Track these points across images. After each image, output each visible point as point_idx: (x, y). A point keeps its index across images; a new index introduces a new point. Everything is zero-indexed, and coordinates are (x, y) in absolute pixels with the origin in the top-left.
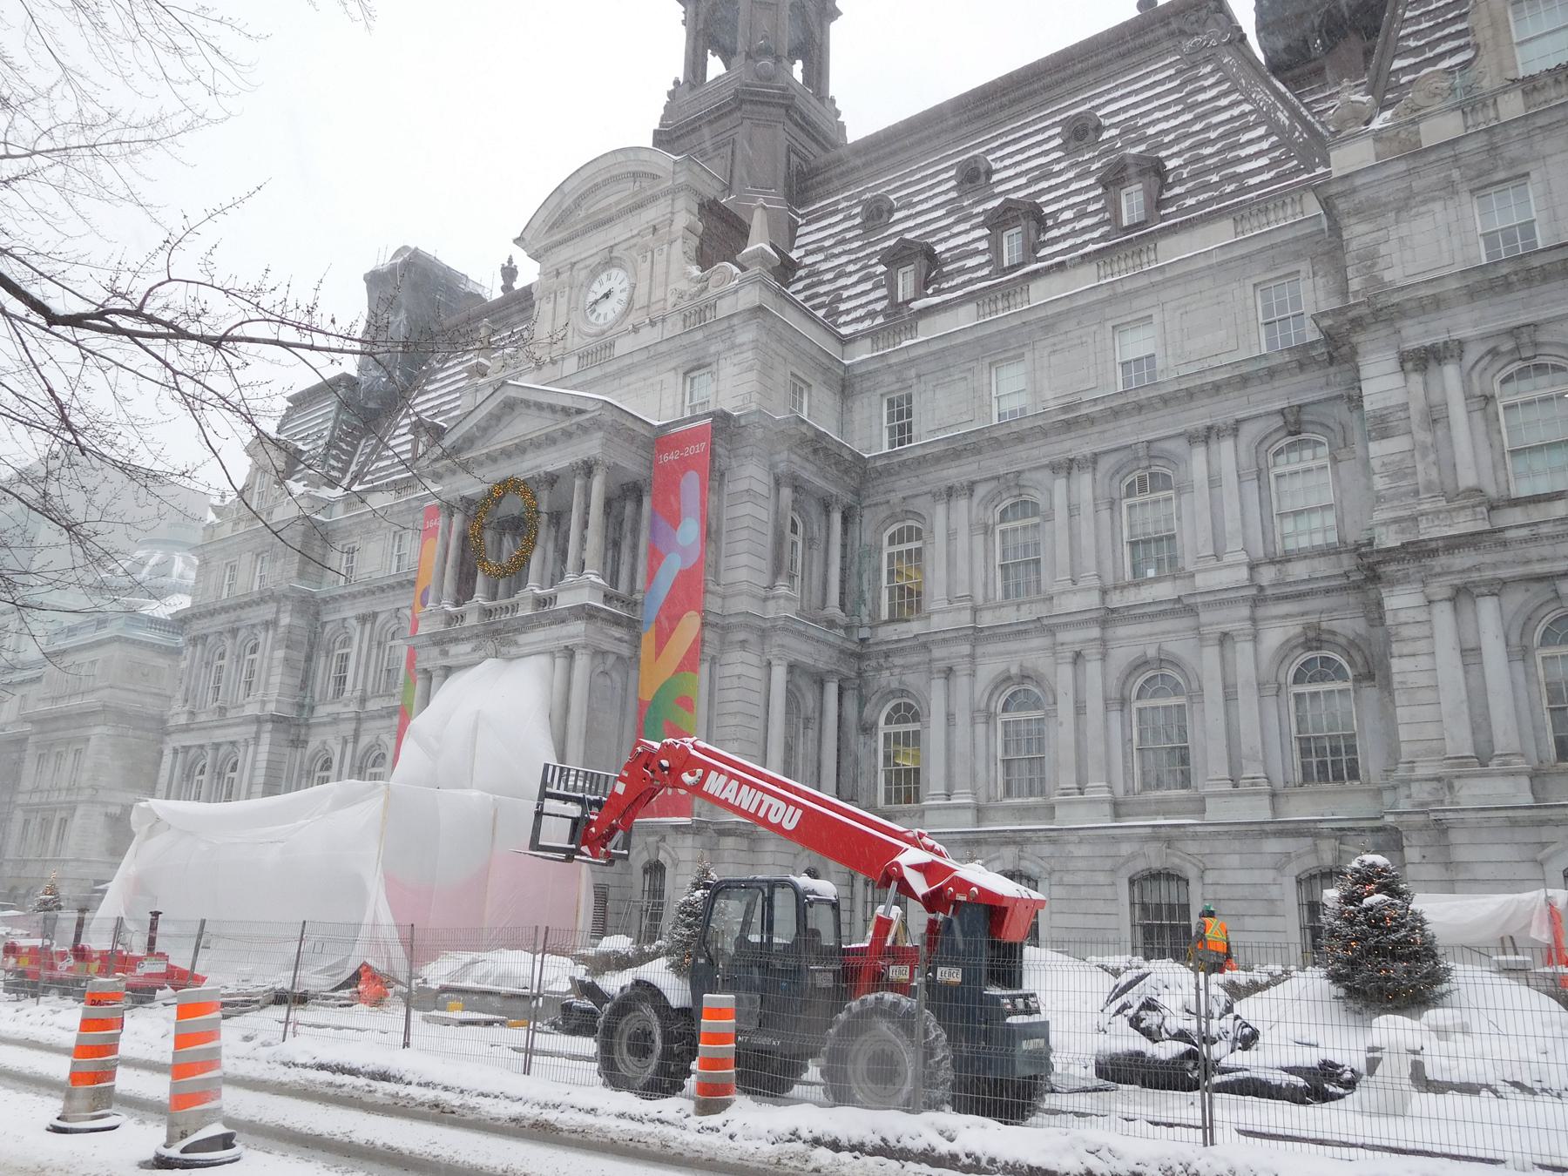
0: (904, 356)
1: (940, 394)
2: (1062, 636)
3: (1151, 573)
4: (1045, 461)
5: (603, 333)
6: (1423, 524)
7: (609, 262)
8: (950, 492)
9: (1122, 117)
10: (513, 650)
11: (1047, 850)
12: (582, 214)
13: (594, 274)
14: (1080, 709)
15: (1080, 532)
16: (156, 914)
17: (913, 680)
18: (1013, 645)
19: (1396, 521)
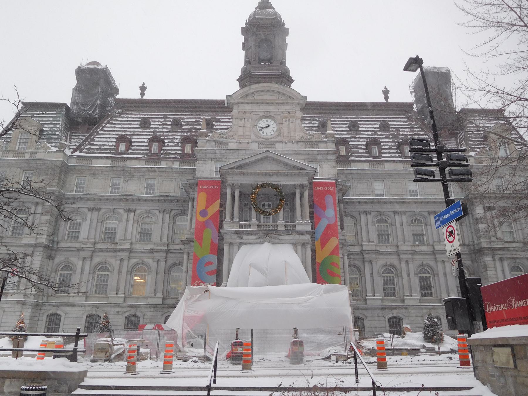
0: (349, 172)
1: (359, 185)
2: (401, 256)
3: (417, 243)
4: (393, 210)
5: (269, 139)
6: (493, 244)
7: (267, 116)
8: (366, 213)
9: (396, 126)
10: (277, 241)
11: (404, 311)
12: (255, 97)
13: (261, 118)
14: (409, 275)
15: (403, 229)
16: (295, 328)
17: (358, 263)
18: (386, 257)
19: (486, 242)
